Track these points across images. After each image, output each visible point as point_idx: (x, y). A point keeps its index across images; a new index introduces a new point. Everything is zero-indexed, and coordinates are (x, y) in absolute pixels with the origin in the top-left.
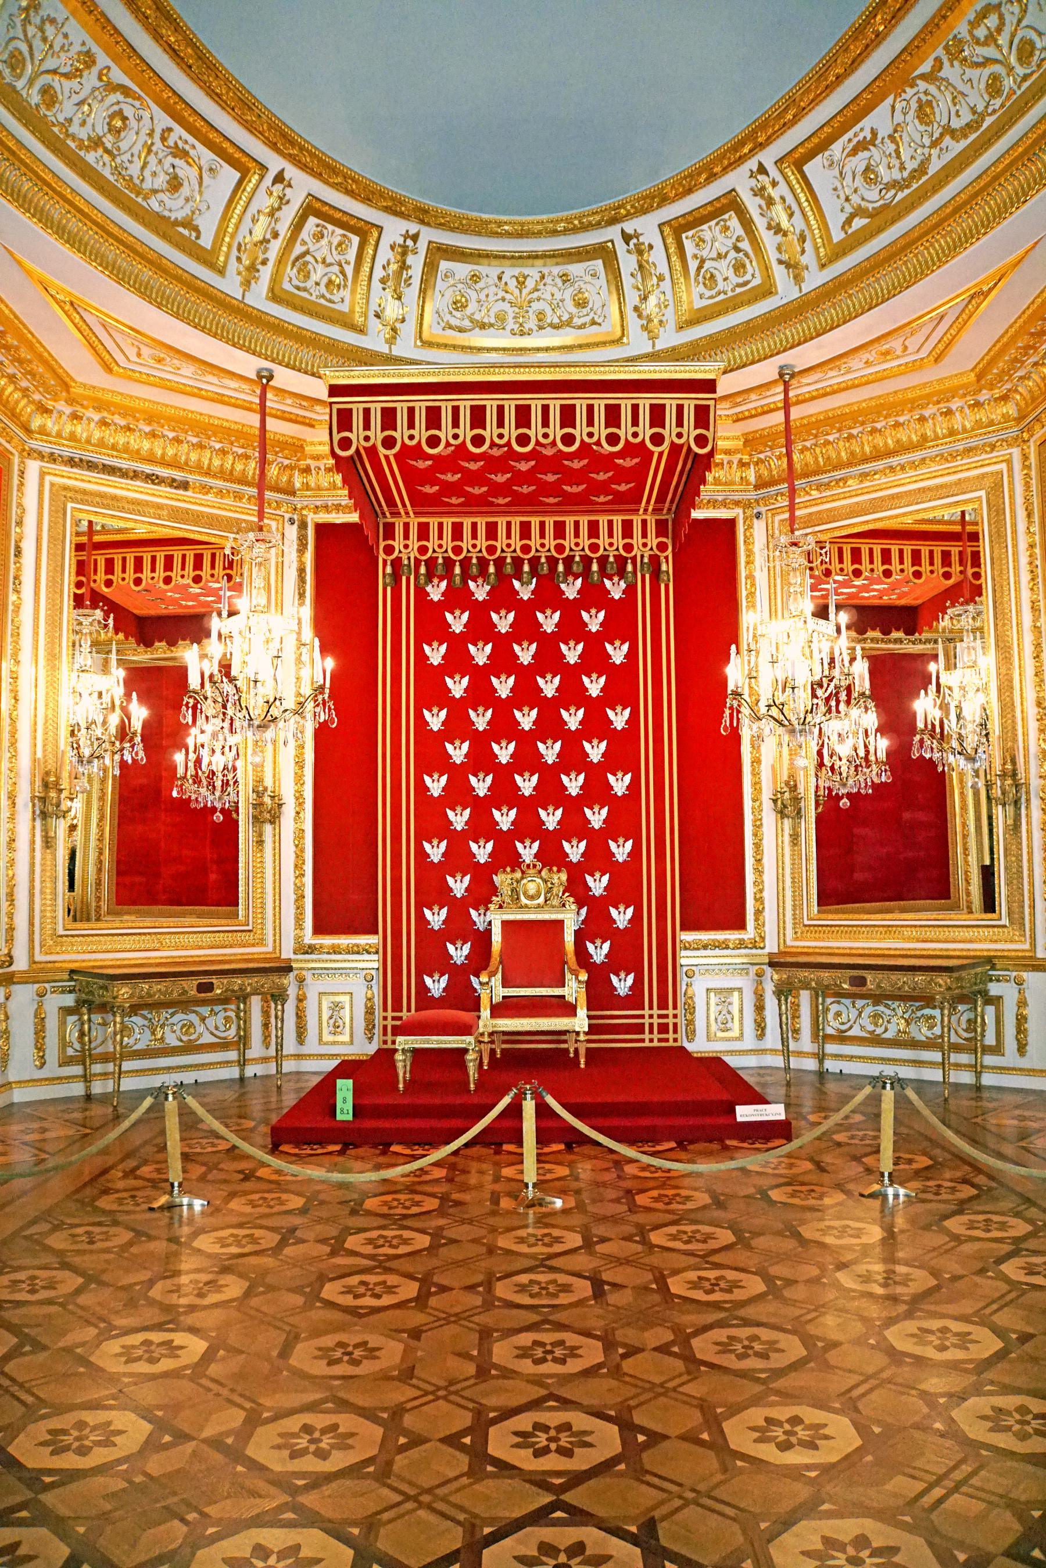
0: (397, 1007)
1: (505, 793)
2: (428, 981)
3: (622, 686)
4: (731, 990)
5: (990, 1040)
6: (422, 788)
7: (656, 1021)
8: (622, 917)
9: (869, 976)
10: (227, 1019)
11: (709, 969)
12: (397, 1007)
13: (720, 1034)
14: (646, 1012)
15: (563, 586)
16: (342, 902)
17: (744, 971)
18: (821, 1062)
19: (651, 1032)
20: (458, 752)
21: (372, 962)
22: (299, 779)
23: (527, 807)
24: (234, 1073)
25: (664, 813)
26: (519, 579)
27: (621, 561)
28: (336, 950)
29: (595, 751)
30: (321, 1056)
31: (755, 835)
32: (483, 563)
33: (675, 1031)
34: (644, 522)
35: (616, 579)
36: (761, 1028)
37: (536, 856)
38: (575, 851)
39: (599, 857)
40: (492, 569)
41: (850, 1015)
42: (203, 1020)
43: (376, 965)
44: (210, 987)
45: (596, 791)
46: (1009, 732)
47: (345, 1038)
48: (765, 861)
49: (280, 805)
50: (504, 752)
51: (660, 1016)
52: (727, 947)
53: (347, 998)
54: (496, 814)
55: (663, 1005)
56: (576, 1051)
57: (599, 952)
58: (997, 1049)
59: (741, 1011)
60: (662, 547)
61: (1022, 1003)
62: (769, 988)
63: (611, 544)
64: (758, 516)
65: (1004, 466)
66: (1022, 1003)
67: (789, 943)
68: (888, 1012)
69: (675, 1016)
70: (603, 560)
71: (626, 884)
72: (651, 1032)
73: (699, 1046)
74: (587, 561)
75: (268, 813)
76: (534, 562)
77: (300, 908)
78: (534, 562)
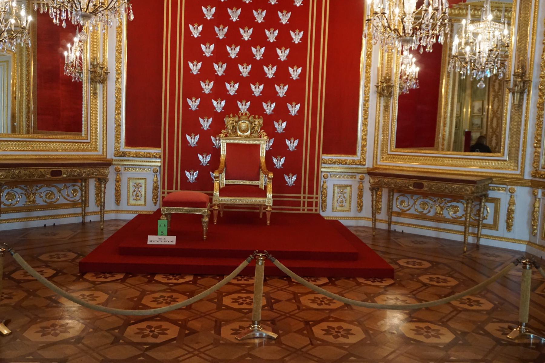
0: (170, 187)
1: (232, 74)
2: (187, 174)
4: (346, 186)
5: (489, 220)
6: (187, 69)
7: (306, 200)
8: (292, 145)
9: (425, 183)
10: (75, 191)
11: (334, 174)
12: (170, 187)
13: (339, 208)
14: (302, 195)
16: (142, 129)
17: (353, 176)
18: (390, 225)
19: (304, 205)
20: (208, 50)
21: (157, 163)
22: (118, 60)
23: (245, 83)
24: (79, 220)
28: (137, 155)
29: (283, 54)
30: (128, 212)
31: (365, 105)
33: (316, 206)
36: (360, 206)
37: (248, 110)
38: (269, 108)
39: (281, 113)
41: (413, 204)
42: (60, 191)
43: (159, 164)
44: (59, 173)
45: (282, 76)
47: (142, 202)
48: (369, 120)
49: (107, 73)
50: (233, 52)
51: (309, 198)
52: (346, 164)
53: (144, 181)
54: (228, 85)
55: (311, 192)
56: (264, 214)
57: (279, 162)
58: (494, 226)
59: (350, 197)
61: (512, 203)
62: (367, 186)
66: (512, 203)
67: (379, 163)
68: (431, 202)
69: (317, 198)
71: (295, 128)
72: (304, 205)
73: (328, 214)
75: (99, 76)
77: (118, 132)
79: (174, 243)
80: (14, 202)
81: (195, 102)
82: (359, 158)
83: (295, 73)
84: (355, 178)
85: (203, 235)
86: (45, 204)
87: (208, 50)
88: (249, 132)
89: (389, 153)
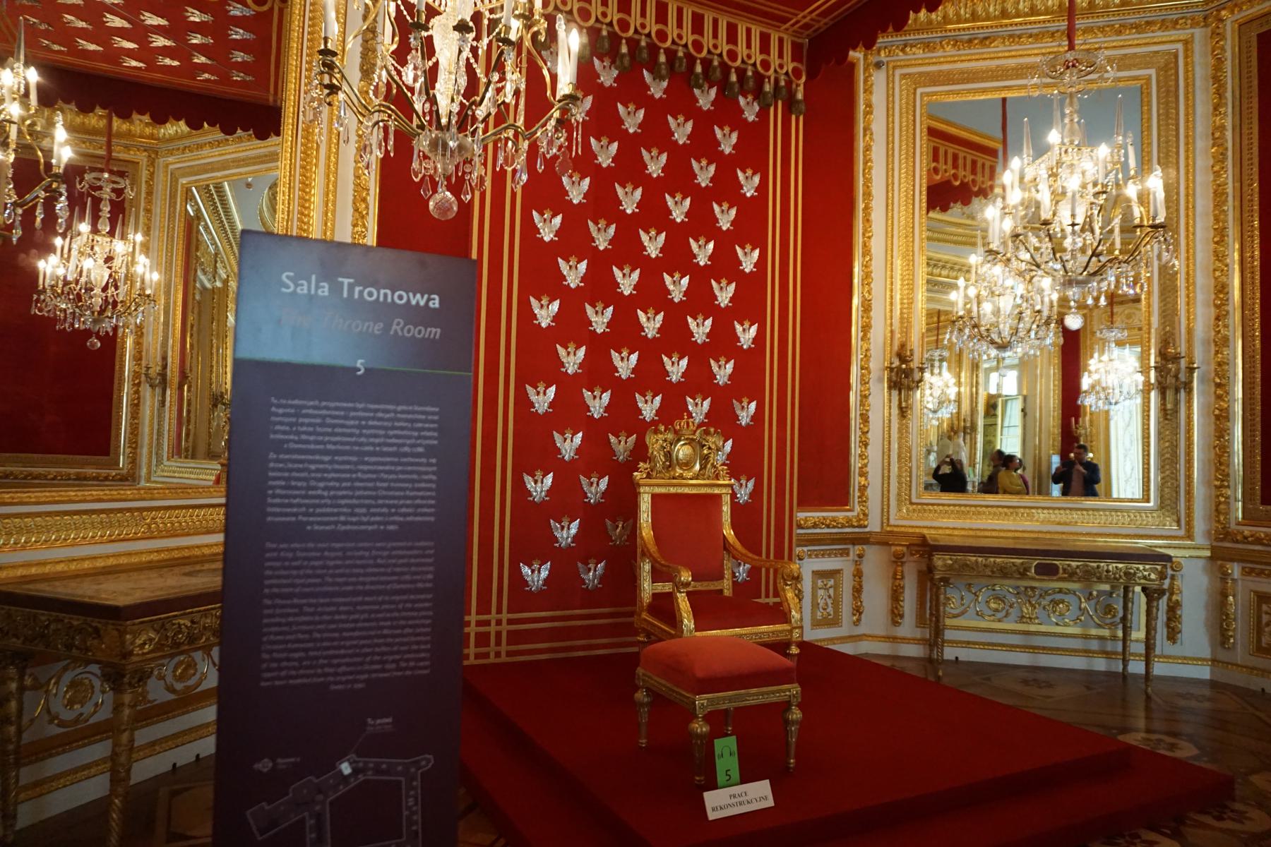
1: (625, 331)
3: (751, 225)
15: (697, 91)
20: (574, 273)
25: (786, 373)
26: (650, 71)
27: (760, 79)
32: (615, 39)
34: (781, 41)
35: (750, 98)
40: (624, 49)
45: (722, 342)
46: (1168, 314)
60: (797, 73)
63: (749, 53)
64: (878, 65)
65: (1180, 46)
70: (741, 73)
74: (725, 69)
76: (671, 54)
78: (671, 54)
79: (770, 803)
80: (89, 708)
81: (545, 394)
82: (855, 514)
83: (746, 335)
84: (848, 555)
85: (788, 756)
86: (172, 697)
87: (574, 273)
88: (697, 467)
89: (914, 500)
